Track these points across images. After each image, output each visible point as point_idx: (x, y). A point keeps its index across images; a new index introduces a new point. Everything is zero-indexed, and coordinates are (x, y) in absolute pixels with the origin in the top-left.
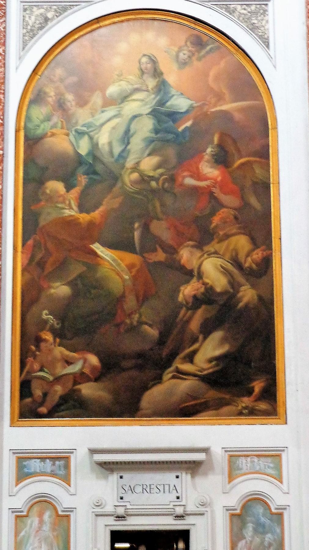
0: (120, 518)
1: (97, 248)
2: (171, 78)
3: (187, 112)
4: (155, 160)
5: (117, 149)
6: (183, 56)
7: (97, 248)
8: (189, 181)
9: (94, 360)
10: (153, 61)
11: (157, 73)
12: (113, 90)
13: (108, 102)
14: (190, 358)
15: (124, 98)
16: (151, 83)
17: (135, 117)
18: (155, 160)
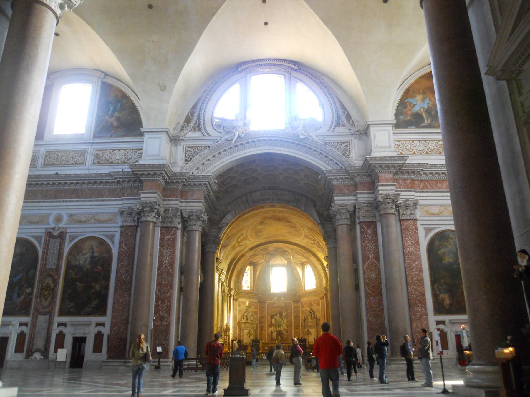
0: (74, 334)
1: (78, 283)
2: (95, 250)
3: (97, 256)
4: (90, 266)
5: (83, 264)
6: (98, 245)
7: (78, 283)
8: (96, 270)
9: (74, 304)
10: (92, 246)
11: (92, 249)
12: (84, 252)
13: (83, 255)
14: (91, 304)
15: (86, 254)
16: (91, 251)
17: (87, 258)
18: (90, 266)
